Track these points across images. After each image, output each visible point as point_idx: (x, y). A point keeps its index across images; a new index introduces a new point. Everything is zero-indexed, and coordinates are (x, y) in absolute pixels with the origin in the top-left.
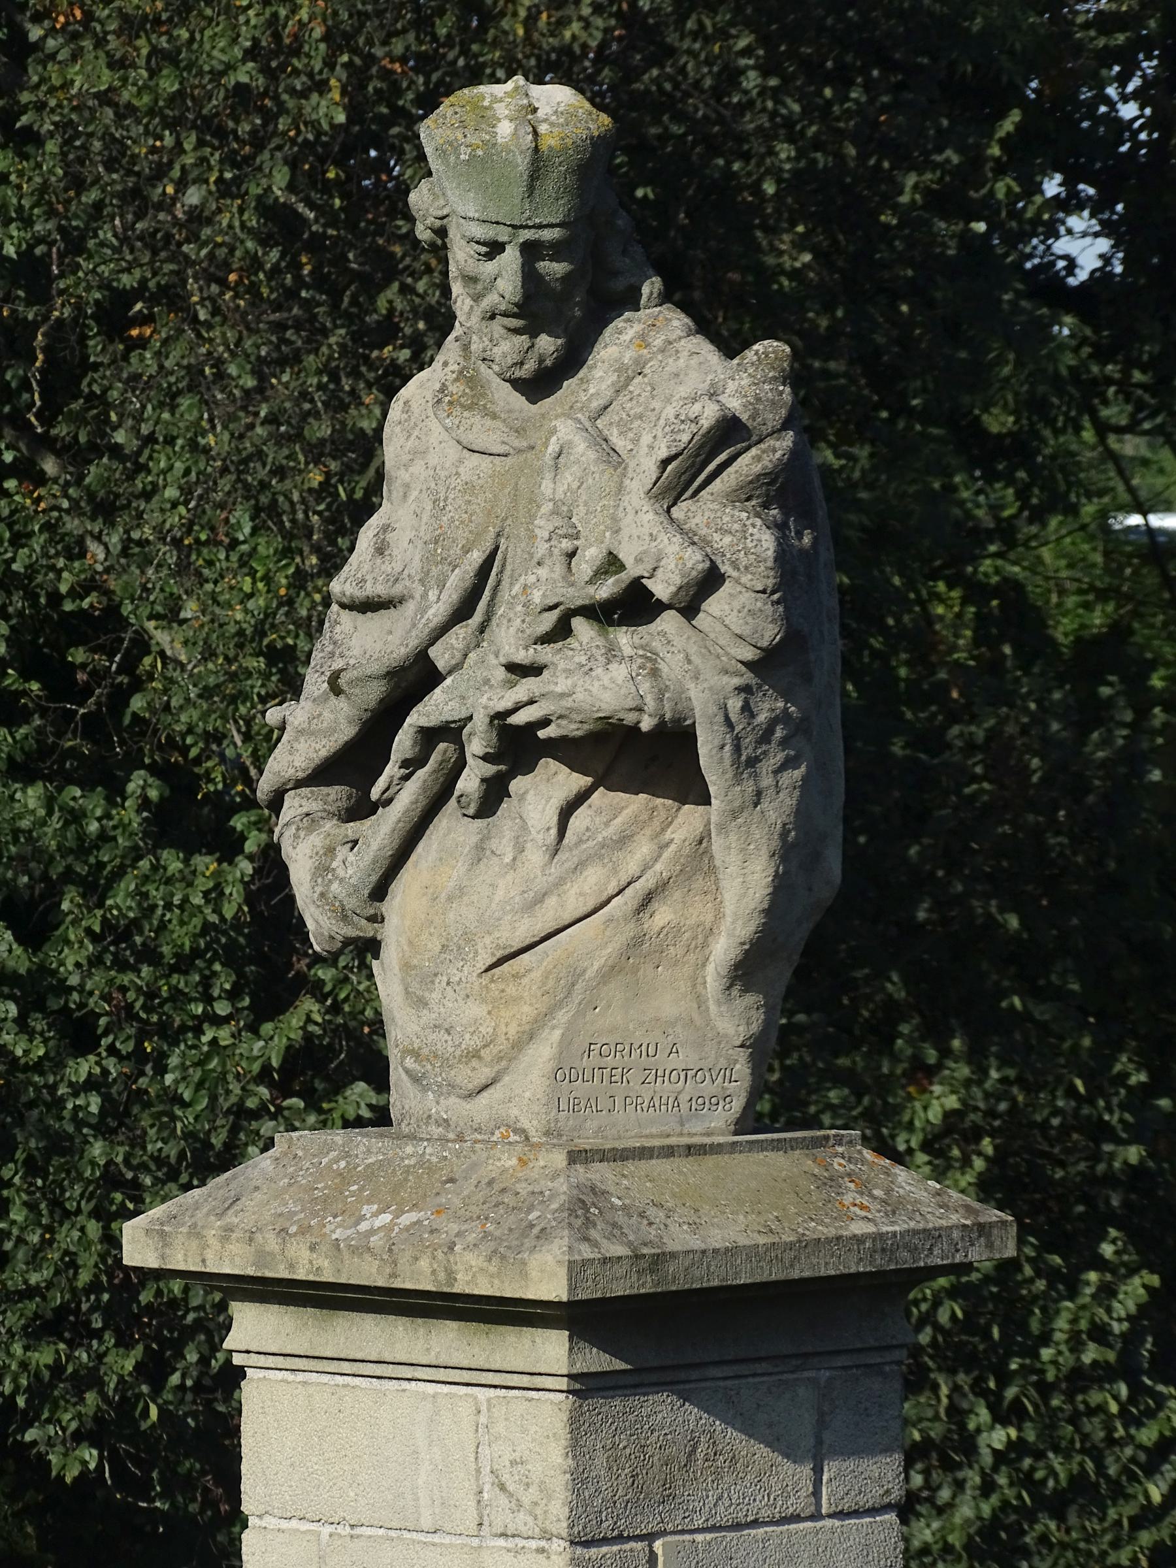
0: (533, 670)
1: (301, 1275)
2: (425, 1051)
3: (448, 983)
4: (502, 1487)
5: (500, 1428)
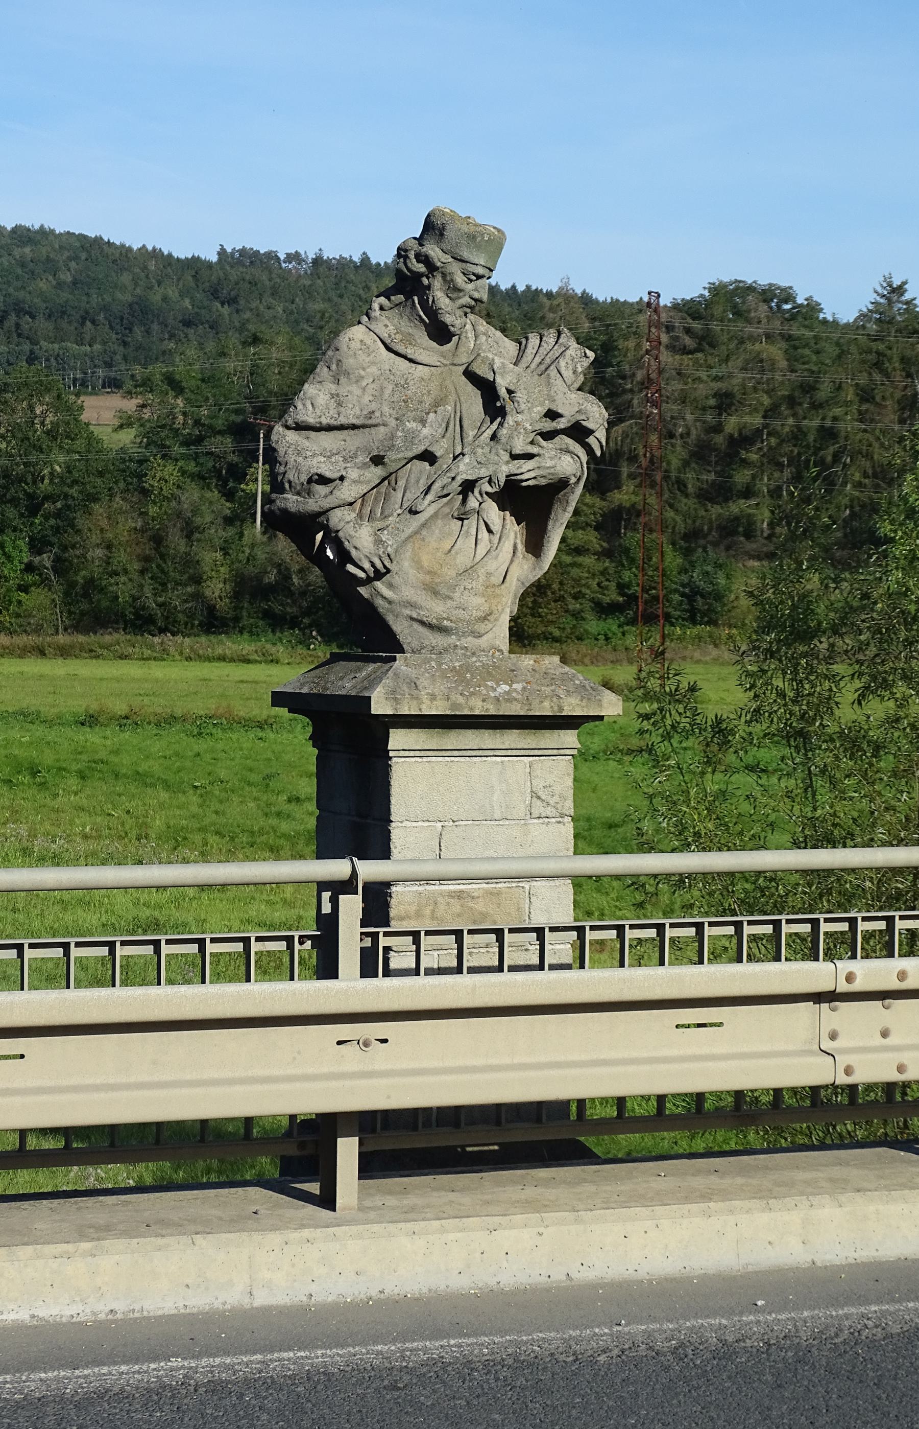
0: (529, 456)
1: (477, 713)
2: (454, 618)
3: (465, 589)
4: (539, 798)
5: (538, 772)
